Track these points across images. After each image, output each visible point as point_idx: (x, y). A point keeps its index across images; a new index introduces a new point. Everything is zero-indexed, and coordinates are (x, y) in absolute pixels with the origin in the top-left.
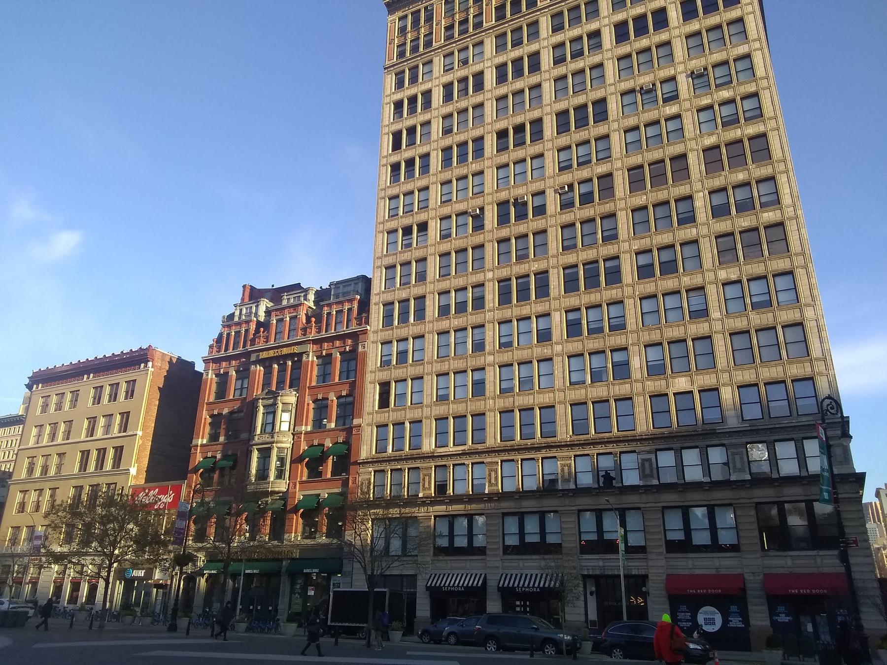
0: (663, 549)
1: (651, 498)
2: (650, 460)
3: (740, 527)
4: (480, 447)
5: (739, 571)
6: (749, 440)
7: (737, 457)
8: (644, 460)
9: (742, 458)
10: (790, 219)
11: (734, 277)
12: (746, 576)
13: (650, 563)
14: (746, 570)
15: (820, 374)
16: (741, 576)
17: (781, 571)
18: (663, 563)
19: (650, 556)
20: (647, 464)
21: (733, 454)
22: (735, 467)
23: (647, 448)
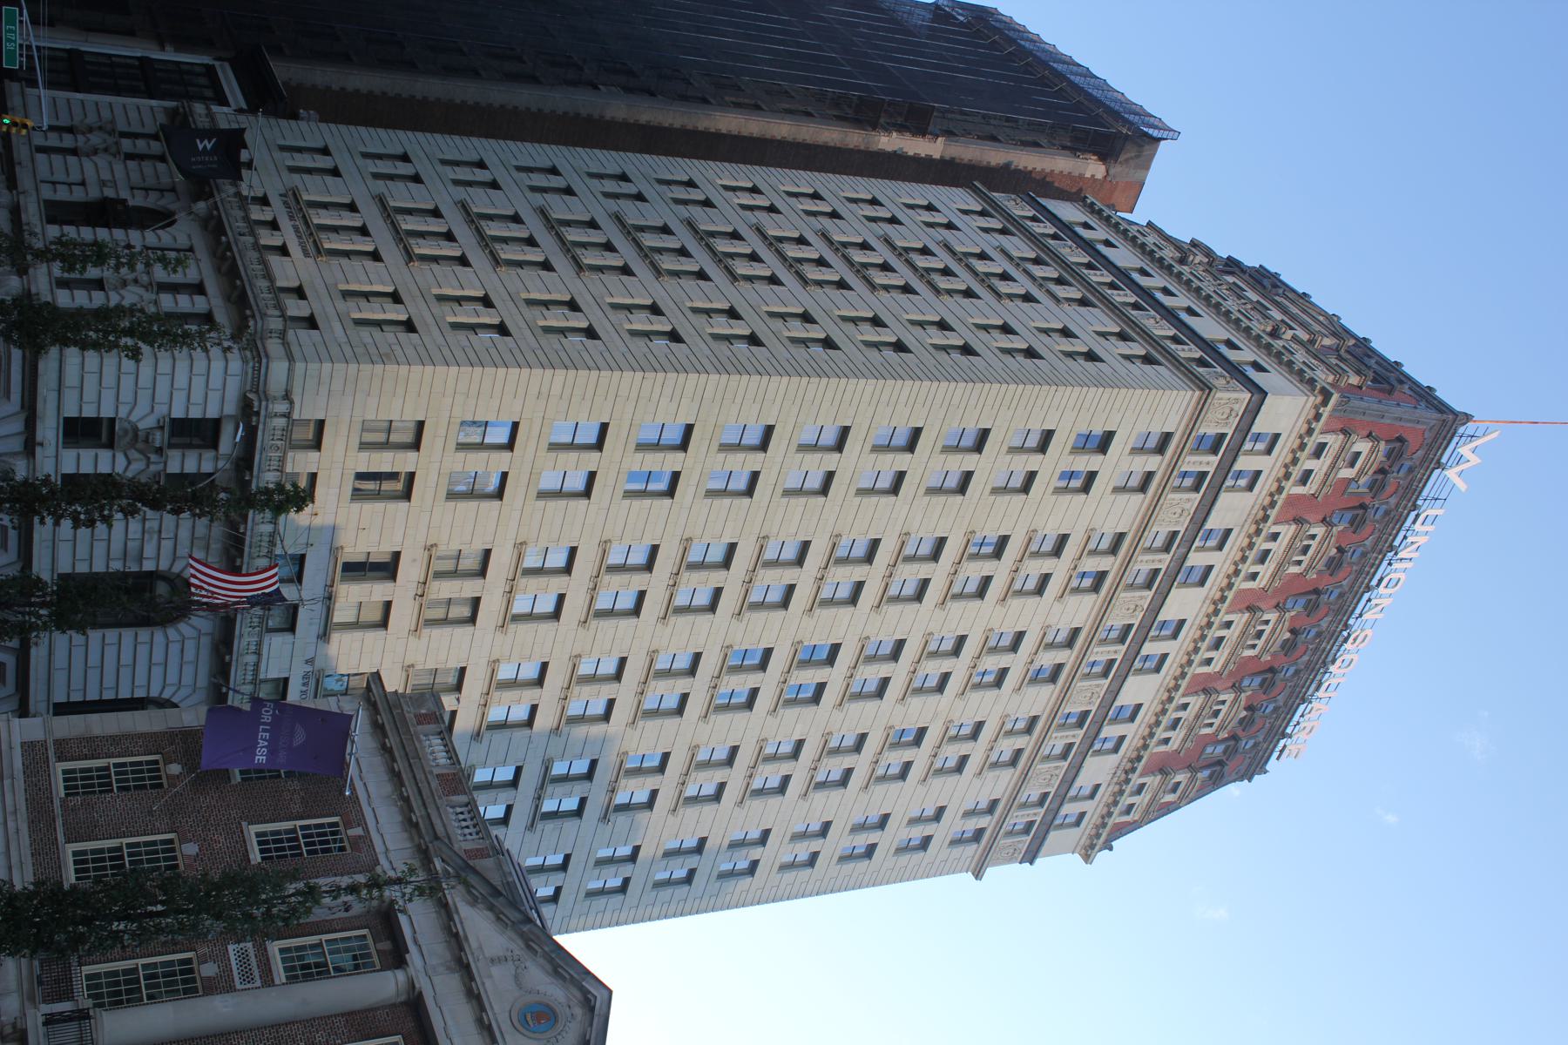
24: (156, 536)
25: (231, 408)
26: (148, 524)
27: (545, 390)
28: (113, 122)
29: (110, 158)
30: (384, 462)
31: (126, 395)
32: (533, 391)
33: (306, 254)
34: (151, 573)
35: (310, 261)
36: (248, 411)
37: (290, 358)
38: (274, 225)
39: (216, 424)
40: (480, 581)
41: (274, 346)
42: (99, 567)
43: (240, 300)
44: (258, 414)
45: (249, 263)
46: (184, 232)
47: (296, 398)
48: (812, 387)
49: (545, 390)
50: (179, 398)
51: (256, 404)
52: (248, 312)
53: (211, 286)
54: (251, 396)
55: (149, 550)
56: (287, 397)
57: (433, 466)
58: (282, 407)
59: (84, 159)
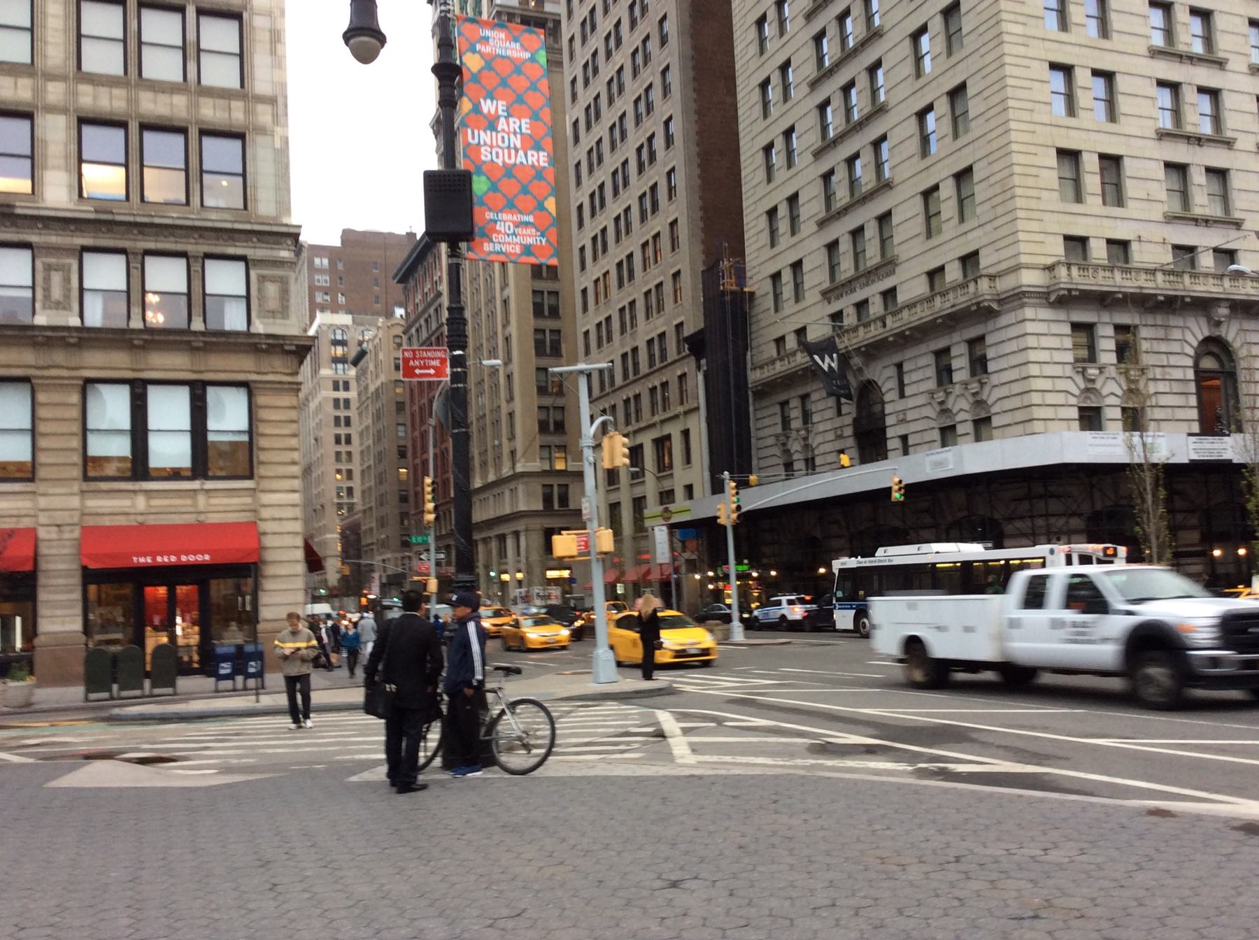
3: (42, 428)
5: (26, 523)
6: (88, 241)
9: (67, 280)
12: (42, 533)
14: (43, 519)
15: (262, 131)
17: (121, 521)
21: (48, 268)
22: (47, 296)
24: (1167, 370)
25: (1062, 315)
26: (1158, 377)
27: (1020, 40)
28: (777, 436)
29: (811, 435)
30: (1092, 182)
31: (1060, 398)
32: (1022, 50)
33: (893, 272)
34: (1196, 372)
35: (897, 270)
36: (1065, 300)
37: (1016, 268)
38: (862, 306)
39: (1076, 327)
40: (1184, 88)
41: (1004, 285)
42: (1194, 414)
43: (954, 320)
44: (1070, 290)
45: (908, 319)
46: (882, 374)
49: (1020, 40)
50: (1058, 356)
51: (1062, 292)
52: (974, 308)
53: (941, 343)
54: (1053, 298)
55: (1178, 374)
56: (1050, 268)
57: (1092, 137)
58: (1062, 272)
59: (816, 452)
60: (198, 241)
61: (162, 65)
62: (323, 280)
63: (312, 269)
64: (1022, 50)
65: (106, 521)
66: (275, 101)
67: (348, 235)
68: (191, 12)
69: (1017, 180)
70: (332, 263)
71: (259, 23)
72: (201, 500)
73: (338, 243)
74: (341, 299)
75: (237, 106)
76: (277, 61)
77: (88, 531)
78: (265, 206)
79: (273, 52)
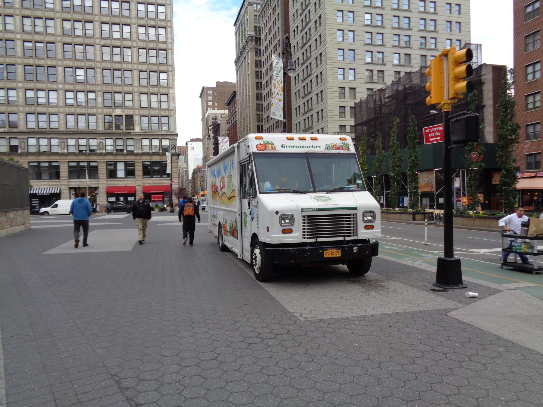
0: (105, 177)
1: (102, 157)
2: (102, 142)
4: (15, 130)
7: (138, 144)
8: (100, 142)
10: (169, 49)
11: (144, 69)
12: (137, 187)
13: (100, 182)
15: (171, 116)
16: (134, 187)
18: (105, 182)
19: (100, 180)
20: (101, 144)
21: (137, 142)
23: (102, 138)
32: (332, 85)
47: (334, 131)
48: (328, 22)
60: (161, 137)
61: (154, 105)
62: (210, 98)
63: (207, 95)
64: (332, 85)
65: (146, 185)
66: (174, 110)
67: (218, 83)
68: (159, 95)
69: (328, 114)
70: (213, 93)
71: (171, 96)
72: (162, 181)
73: (215, 86)
74: (216, 104)
75: (167, 111)
76: (174, 103)
77: (144, 187)
78: (172, 130)
79: (173, 101)
